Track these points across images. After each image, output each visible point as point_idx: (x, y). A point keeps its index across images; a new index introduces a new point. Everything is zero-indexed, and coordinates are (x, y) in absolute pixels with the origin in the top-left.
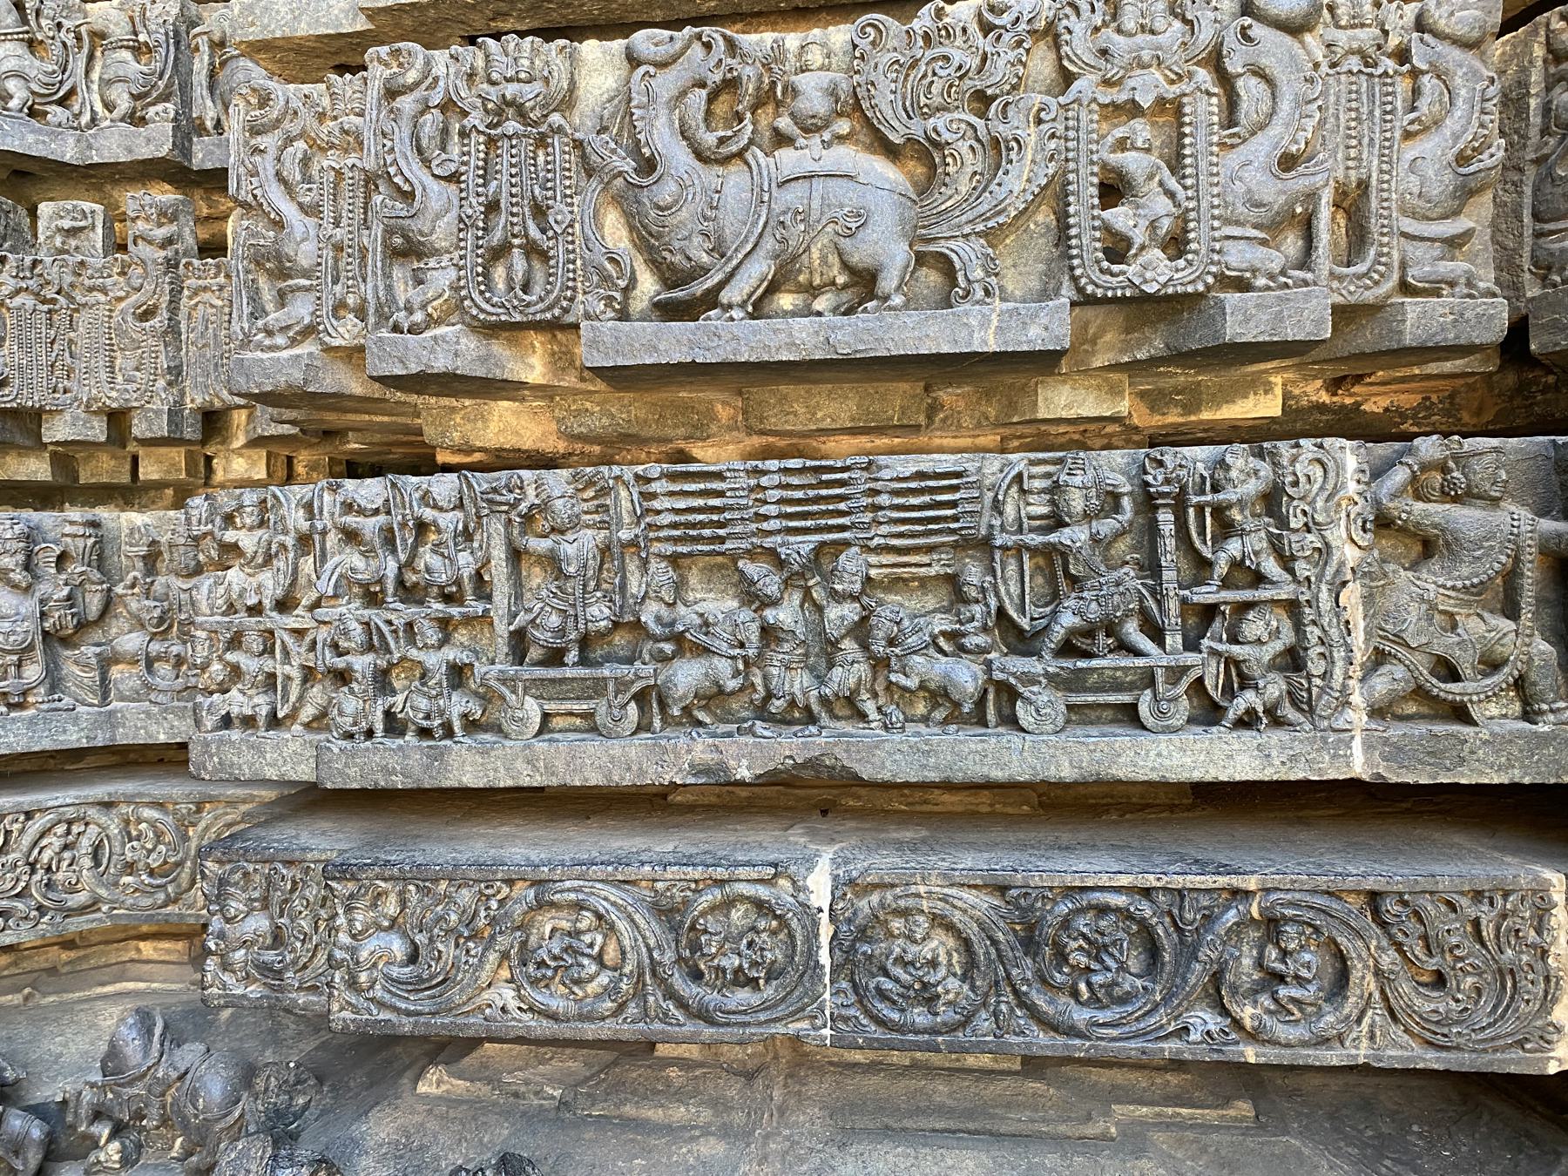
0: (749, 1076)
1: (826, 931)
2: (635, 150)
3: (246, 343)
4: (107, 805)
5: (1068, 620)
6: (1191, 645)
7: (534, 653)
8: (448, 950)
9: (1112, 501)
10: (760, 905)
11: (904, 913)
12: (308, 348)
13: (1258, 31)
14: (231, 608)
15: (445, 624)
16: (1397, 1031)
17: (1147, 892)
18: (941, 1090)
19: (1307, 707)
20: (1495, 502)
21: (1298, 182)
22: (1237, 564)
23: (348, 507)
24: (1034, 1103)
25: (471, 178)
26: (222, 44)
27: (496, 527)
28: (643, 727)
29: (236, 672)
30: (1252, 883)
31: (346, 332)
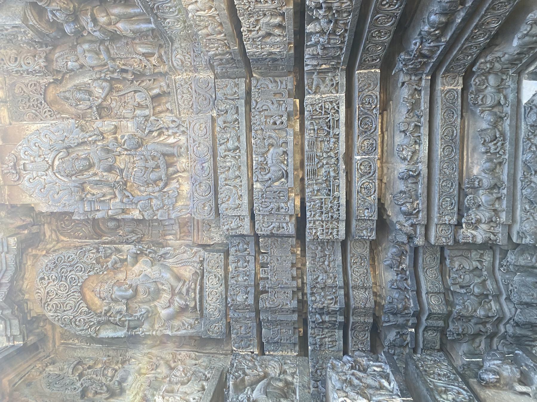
0: (388, 169)
1: (364, 157)
2: (268, 181)
3: (289, 232)
4: (351, 267)
5: (326, 128)
6: (329, 114)
7: (329, 193)
8: (366, 204)
9: (312, 123)
10: (361, 165)
11: (361, 147)
12: (289, 224)
13: (257, 107)
14: (323, 234)
15: (325, 204)
16: (376, 89)
17: (359, 118)
18: (389, 142)
19: (337, 101)
20: (313, 79)
21: (275, 102)
22: (320, 109)
23: (310, 216)
24: (390, 130)
25: (270, 201)
26: (236, 251)
27: (313, 197)
28: (338, 179)
29: (331, 233)
30: (357, 106)
31: (287, 218)
